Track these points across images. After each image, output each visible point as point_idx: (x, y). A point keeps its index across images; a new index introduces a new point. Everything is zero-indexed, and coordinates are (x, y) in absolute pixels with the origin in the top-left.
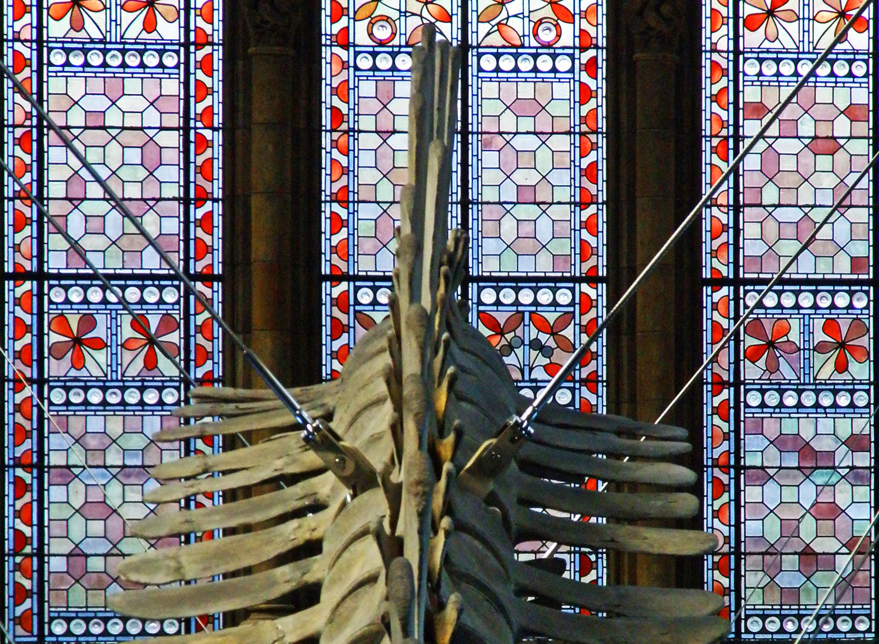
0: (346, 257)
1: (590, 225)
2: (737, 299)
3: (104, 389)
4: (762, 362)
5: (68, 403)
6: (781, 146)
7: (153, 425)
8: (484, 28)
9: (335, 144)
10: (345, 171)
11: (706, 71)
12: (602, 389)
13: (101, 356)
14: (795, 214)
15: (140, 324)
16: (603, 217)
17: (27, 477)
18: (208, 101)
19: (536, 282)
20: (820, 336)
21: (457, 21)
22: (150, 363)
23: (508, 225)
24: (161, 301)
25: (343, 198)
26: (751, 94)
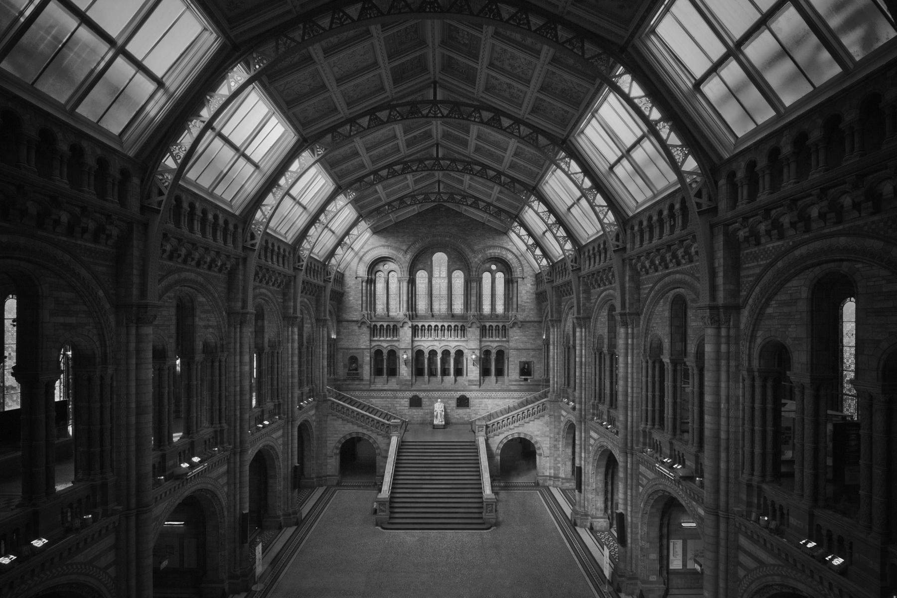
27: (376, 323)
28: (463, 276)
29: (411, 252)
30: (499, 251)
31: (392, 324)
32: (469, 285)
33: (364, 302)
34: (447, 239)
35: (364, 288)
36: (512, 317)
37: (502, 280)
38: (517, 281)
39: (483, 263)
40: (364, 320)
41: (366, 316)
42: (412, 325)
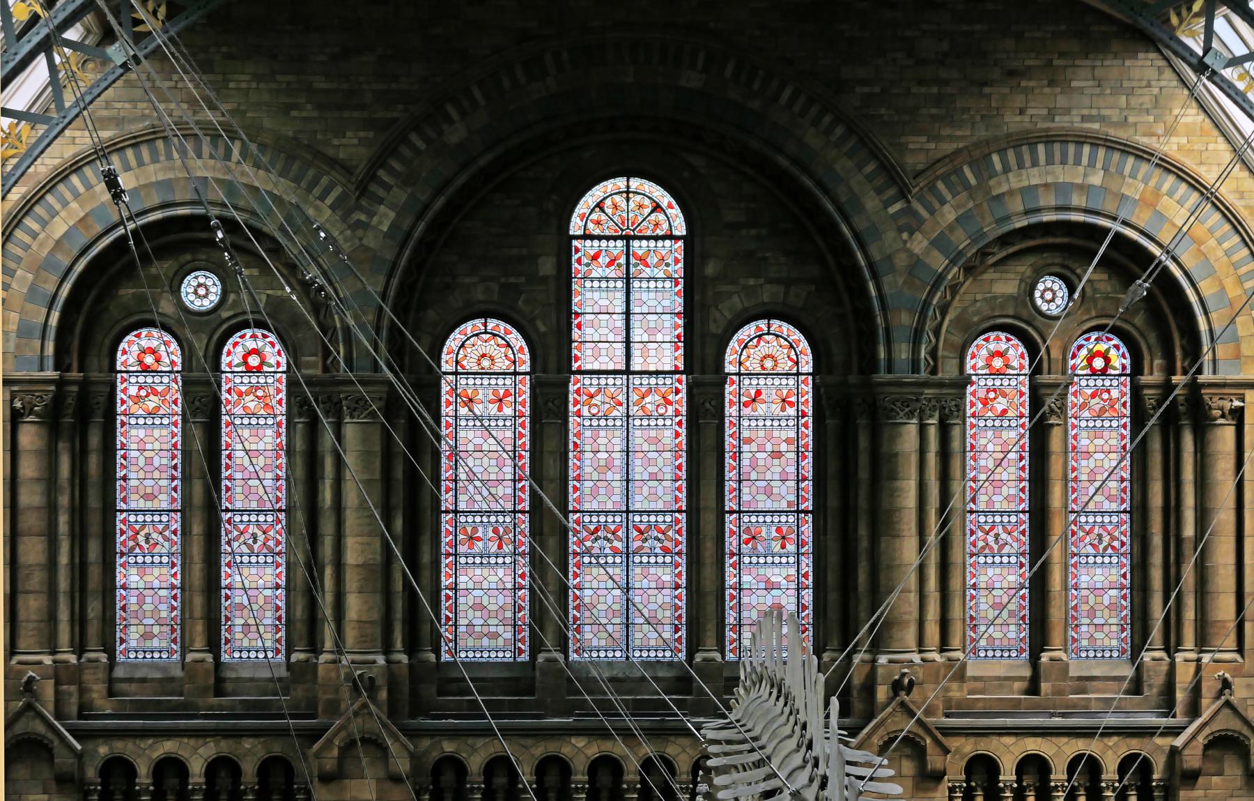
0: (579, 503)
1: (679, 489)
2: (740, 519)
3: (482, 557)
4: (750, 545)
5: (467, 563)
6: (758, 455)
7: (501, 572)
8: (636, 408)
9: (575, 457)
10: (579, 468)
11: (727, 425)
12: (684, 557)
13: (480, 544)
14: (764, 484)
15: (495, 531)
16: (684, 485)
17: (451, 594)
18: (523, 440)
19: (657, 512)
20: (774, 534)
21: (625, 406)
22: (500, 547)
23: (645, 489)
24: (504, 522)
25: (578, 479)
26: (745, 434)
27: (124, 748)
28: (807, 366)
29: (407, 180)
30: (1096, 179)
31: (250, 755)
32: (863, 442)
33: (36, 580)
34: (692, 80)
35: (29, 468)
36: (1196, 691)
37: (1119, 391)
38: (1238, 416)
39: (969, 270)
40: (40, 728)
41: (48, 690)
42: (413, 756)
